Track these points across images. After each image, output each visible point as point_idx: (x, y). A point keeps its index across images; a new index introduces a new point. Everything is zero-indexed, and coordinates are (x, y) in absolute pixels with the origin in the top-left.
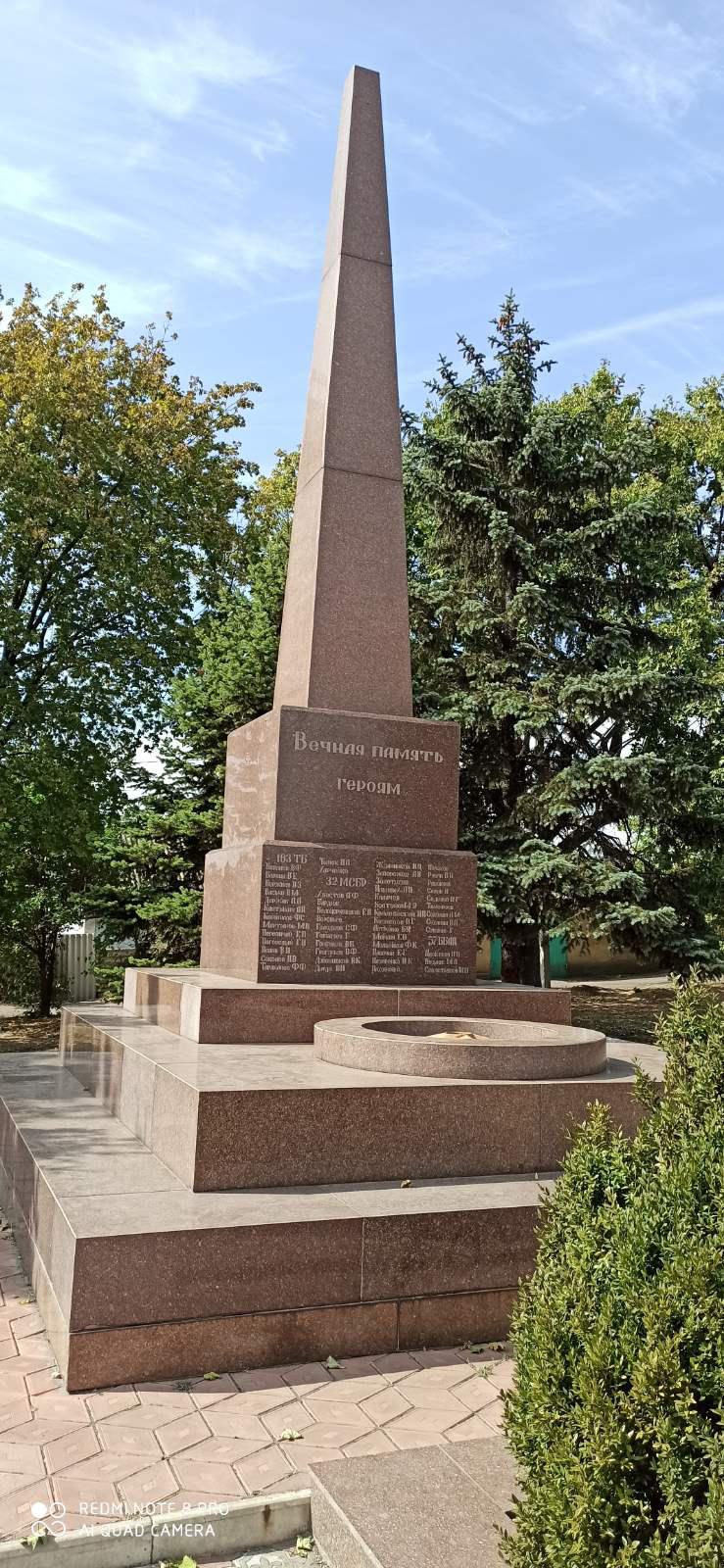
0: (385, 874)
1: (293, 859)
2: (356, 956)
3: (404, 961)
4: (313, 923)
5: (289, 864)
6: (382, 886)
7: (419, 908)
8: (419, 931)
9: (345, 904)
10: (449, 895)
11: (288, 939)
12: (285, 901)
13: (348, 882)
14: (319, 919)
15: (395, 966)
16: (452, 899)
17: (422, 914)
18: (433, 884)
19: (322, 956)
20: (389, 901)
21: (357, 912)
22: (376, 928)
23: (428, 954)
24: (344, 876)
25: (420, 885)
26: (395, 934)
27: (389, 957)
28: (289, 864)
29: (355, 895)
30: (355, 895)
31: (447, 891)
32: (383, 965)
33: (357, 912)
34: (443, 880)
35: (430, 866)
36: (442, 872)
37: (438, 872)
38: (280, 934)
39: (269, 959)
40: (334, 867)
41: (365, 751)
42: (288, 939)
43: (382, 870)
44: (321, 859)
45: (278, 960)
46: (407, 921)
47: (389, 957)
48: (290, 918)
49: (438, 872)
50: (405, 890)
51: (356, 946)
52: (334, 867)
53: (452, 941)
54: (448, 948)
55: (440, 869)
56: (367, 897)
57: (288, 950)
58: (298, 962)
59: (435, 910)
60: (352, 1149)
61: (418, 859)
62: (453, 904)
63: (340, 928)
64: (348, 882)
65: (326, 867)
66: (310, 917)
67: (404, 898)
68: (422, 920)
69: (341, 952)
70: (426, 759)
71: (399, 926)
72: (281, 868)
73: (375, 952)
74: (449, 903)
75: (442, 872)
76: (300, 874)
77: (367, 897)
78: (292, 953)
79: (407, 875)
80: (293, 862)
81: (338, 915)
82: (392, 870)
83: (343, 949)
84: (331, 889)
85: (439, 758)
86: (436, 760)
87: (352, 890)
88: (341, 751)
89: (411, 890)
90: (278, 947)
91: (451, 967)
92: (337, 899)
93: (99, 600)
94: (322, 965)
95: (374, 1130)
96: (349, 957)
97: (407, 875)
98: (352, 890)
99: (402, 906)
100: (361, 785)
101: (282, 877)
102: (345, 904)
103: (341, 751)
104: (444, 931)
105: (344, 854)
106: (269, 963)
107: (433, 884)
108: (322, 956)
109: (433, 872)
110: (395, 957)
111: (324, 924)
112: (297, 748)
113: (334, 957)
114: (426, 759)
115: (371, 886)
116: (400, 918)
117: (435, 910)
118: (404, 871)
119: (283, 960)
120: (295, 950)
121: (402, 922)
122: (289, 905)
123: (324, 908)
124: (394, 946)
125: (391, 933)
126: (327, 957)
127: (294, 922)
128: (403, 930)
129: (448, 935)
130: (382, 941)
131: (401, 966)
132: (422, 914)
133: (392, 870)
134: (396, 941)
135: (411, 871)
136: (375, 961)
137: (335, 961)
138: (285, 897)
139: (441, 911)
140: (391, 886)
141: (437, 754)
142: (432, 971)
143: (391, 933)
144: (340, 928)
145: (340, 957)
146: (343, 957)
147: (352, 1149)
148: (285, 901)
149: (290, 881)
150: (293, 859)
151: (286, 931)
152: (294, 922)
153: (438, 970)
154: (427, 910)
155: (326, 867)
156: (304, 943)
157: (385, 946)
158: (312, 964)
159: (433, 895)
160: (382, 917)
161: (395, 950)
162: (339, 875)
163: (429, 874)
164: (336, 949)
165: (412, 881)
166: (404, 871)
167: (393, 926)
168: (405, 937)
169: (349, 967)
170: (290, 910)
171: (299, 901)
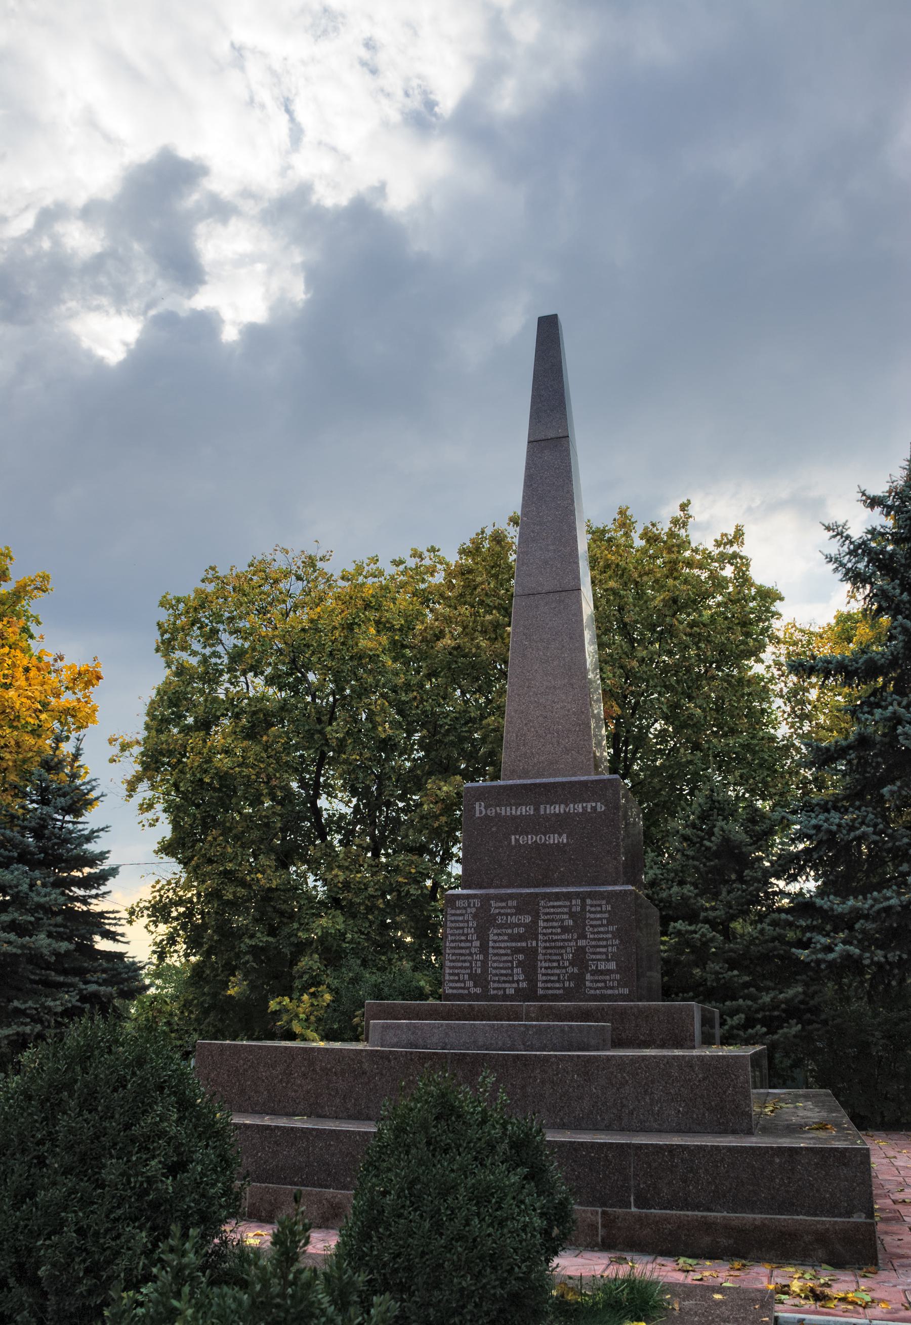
0: (547, 910)
1: (469, 904)
2: (523, 981)
3: (567, 984)
4: (486, 955)
5: (465, 908)
6: (544, 921)
7: (579, 938)
8: (580, 958)
9: (513, 938)
10: (607, 926)
11: (466, 968)
12: (463, 938)
13: (514, 919)
14: (491, 951)
15: (559, 988)
16: (611, 928)
17: (582, 943)
18: (592, 916)
19: (494, 982)
20: (552, 934)
21: (524, 944)
22: (540, 957)
23: (588, 977)
24: (511, 915)
25: (579, 918)
26: (558, 961)
27: (553, 982)
28: (465, 908)
29: (522, 930)
30: (522, 930)
31: (605, 922)
32: (548, 988)
33: (524, 944)
34: (601, 912)
35: (588, 901)
36: (600, 906)
37: (596, 906)
38: (459, 964)
39: (451, 985)
40: (502, 908)
41: (535, 810)
42: (466, 968)
43: (544, 907)
44: (492, 902)
45: (458, 985)
46: (569, 950)
47: (553, 982)
48: (468, 951)
49: (596, 906)
50: (566, 923)
51: (523, 972)
52: (502, 908)
53: (612, 966)
54: (609, 972)
55: (598, 902)
56: (532, 931)
57: (466, 977)
58: (475, 987)
59: (594, 939)
60: (296, 1091)
61: (577, 895)
62: (612, 932)
63: (510, 958)
64: (514, 919)
65: (496, 908)
66: (484, 949)
67: (565, 929)
68: (583, 948)
69: (511, 978)
70: (589, 810)
71: (562, 955)
72: (458, 912)
73: (540, 977)
74: (607, 932)
75: (600, 906)
76: (475, 916)
77: (532, 931)
78: (469, 980)
79: (566, 910)
80: (469, 906)
81: (507, 948)
82: (553, 907)
83: (512, 975)
84: (500, 926)
85: (601, 808)
86: (599, 810)
87: (518, 925)
88: (514, 812)
89: (571, 922)
90: (458, 974)
91: (612, 988)
92: (505, 934)
93: (202, 699)
94: (494, 989)
95: (312, 1079)
96: (518, 982)
97: (566, 910)
98: (518, 925)
99: (563, 937)
100: (532, 838)
101: (461, 918)
102: (513, 938)
103: (514, 812)
104: (604, 957)
105: (511, 896)
106: (451, 988)
107: (592, 916)
108: (494, 982)
109: (591, 906)
110: (558, 981)
111: (495, 955)
112: (477, 815)
113: (505, 982)
114: (589, 810)
115: (535, 922)
116: (562, 947)
117: (594, 939)
118: (565, 907)
119: (462, 985)
120: (472, 977)
121: (563, 951)
122: (467, 941)
123: (495, 941)
124: (557, 971)
125: (554, 961)
126: (499, 982)
127: (471, 954)
128: (565, 957)
129: (608, 960)
130: (546, 968)
131: (564, 988)
132: (582, 943)
133: (553, 907)
134: (559, 967)
135: (570, 907)
136: (540, 985)
137: (507, 985)
138: (463, 934)
139: (599, 940)
140: (553, 920)
141: (599, 804)
142: (592, 992)
143: (554, 961)
144: (510, 958)
145: (509, 982)
146: (513, 982)
147: (296, 1091)
148: (463, 938)
149: (467, 922)
150: (469, 904)
151: (465, 961)
152: (471, 954)
153: (598, 992)
154: (586, 938)
155: (496, 908)
156: (479, 971)
157: (549, 971)
158: (485, 988)
159: (591, 926)
160: (545, 948)
161: (559, 975)
162: (507, 915)
163: (588, 908)
164: (506, 975)
165: (572, 915)
166: (565, 907)
167: (556, 954)
168: (567, 964)
169: (517, 990)
170: (469, 944)
171: (475, 937)
